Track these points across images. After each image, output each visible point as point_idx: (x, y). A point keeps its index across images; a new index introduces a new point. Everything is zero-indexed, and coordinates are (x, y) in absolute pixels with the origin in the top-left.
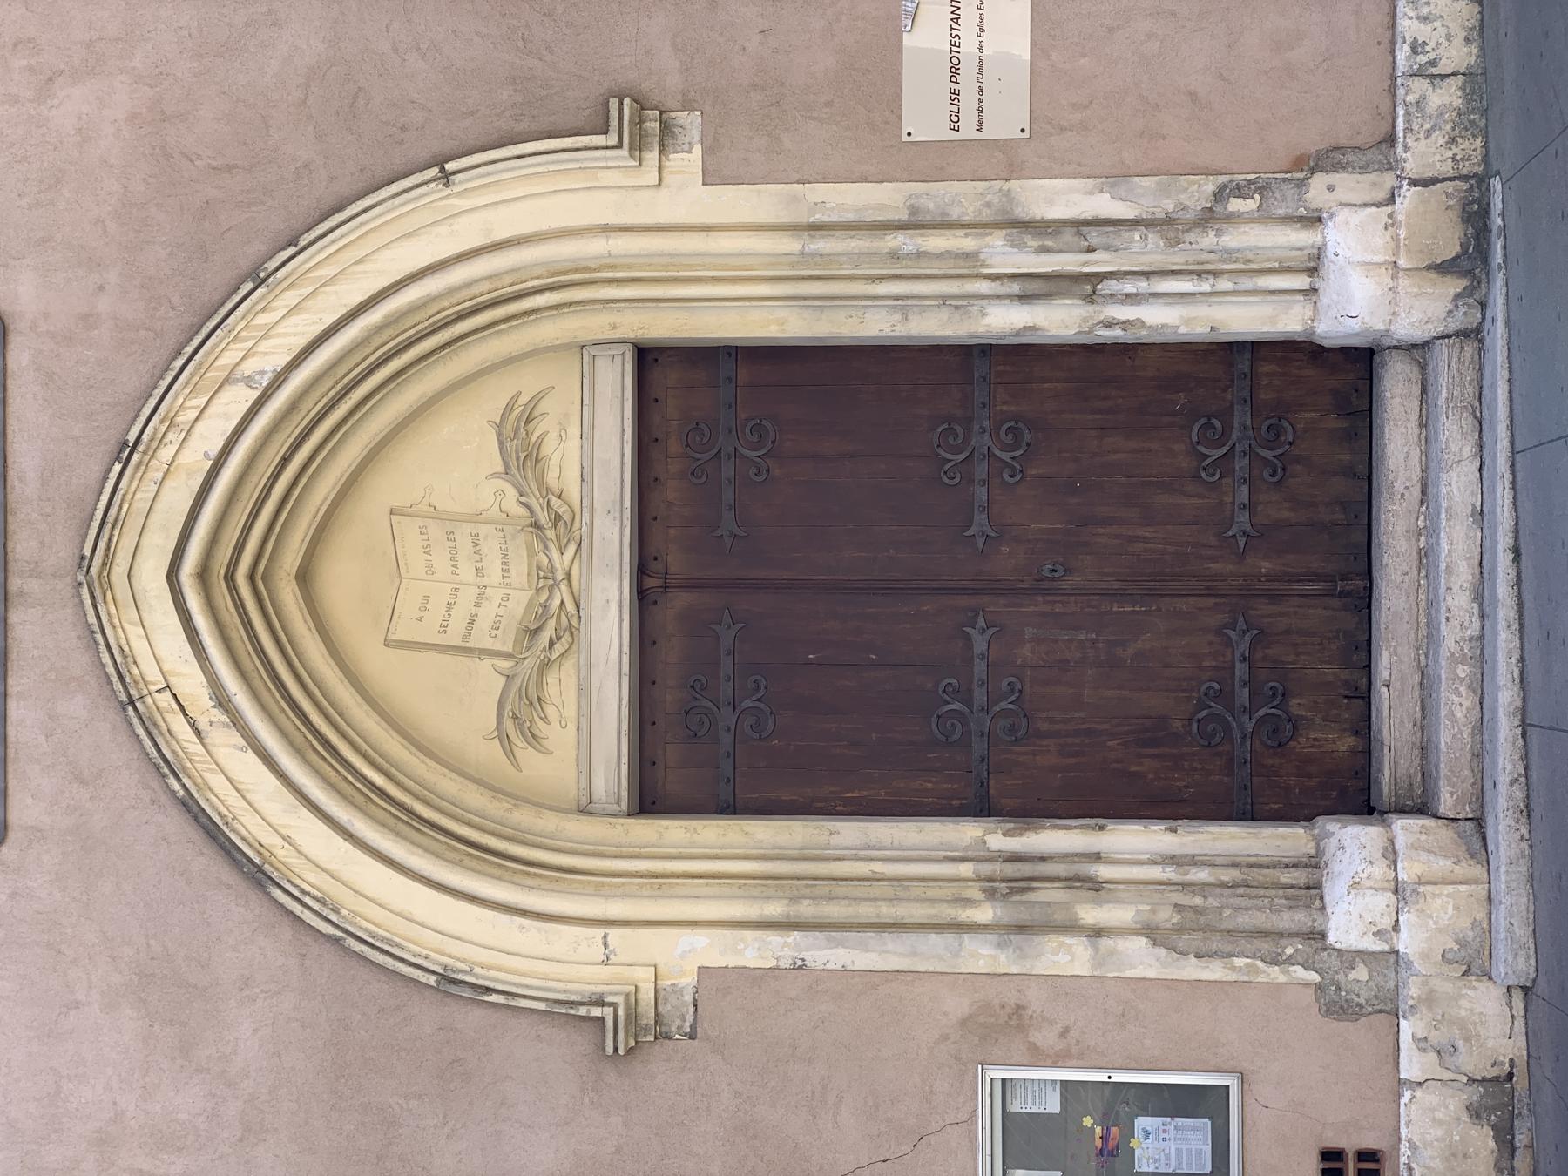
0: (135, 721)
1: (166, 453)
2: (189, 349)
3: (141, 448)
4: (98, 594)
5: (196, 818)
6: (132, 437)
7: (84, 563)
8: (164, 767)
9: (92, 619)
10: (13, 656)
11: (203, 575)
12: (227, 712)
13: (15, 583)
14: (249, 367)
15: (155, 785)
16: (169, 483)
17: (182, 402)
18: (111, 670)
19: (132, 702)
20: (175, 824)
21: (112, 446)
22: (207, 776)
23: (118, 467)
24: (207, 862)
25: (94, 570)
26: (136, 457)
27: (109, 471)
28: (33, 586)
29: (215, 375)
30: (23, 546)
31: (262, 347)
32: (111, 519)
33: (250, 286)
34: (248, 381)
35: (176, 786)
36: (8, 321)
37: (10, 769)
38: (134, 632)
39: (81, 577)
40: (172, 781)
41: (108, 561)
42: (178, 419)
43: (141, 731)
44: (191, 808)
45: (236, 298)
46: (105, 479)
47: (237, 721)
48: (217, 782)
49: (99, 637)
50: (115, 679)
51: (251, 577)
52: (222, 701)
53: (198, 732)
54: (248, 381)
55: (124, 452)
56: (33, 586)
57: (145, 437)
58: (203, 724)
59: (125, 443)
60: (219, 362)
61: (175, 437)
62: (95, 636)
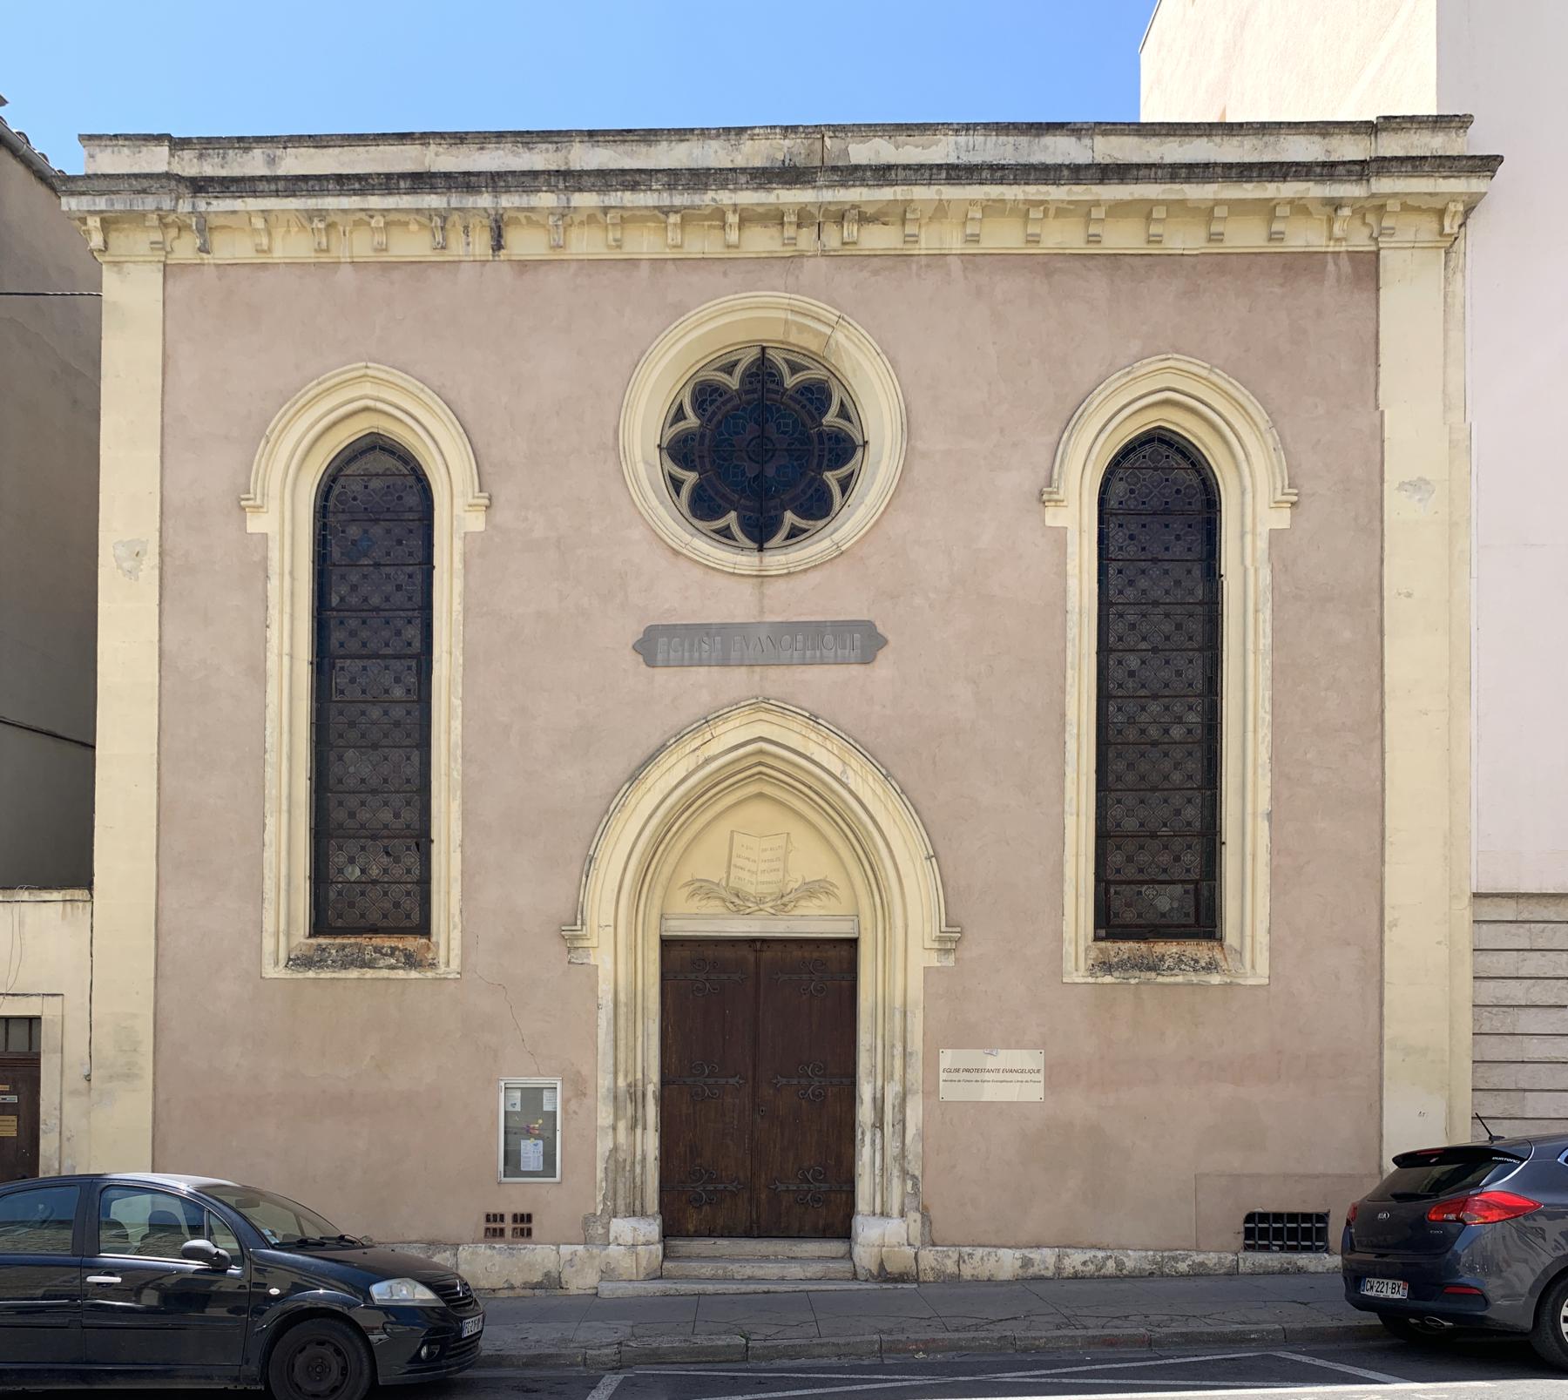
0: (699, 723)
1: (813, 736)
2: (858, 746)
3: (815, 725)
4: (753, 707)
5: (658, 750)
6: (820, 721)
7: (766, 700)
8: (679, 737)
9: (743, 704)
10: (727, 669)
11: (761, 752)
12: (703, 763)
13: (758, 669)
14: (850, 773)
15: (673, 732)
16: (799, 736)
17: (835, 744)
18: (721, 712)
19: (707, 722)
20: (655, 742)
21: (816, 712)
22: (675, 755)
23: (807, 715)
24: (639, 755)
25: (763, 705)
26: (812, 723)
27: (806, 711)
28: (757, 677)
29: (847, 757)
30: (774, 673)
31: (858, 778)
32: (786, 712)
33: (884, 772)
34: (844, 772)
35: (671, 742)
36: (871, 665)
37: (678, 669)
38: (737, 722)
39: (760, 699)
40: (674, 740)
41: (767, 711)
42: (828, 742)
43: (695, 726)
44: (662, 748)
45: (879, 767)
46: (802, 709)
47: (699, 767)
48: (673, 759)
49: (735, 707)
50: (717, 714)
51: (760, 773)
52: (707, 761)
53: (694, 751)
54: (844, 772)
55: (814, 718)
56: (757, 677)
57: (820, 727)
58: (697, 753)
59: (817, 718)
60: (852, 760)
61: (820, 740)
62: (735, 705)
